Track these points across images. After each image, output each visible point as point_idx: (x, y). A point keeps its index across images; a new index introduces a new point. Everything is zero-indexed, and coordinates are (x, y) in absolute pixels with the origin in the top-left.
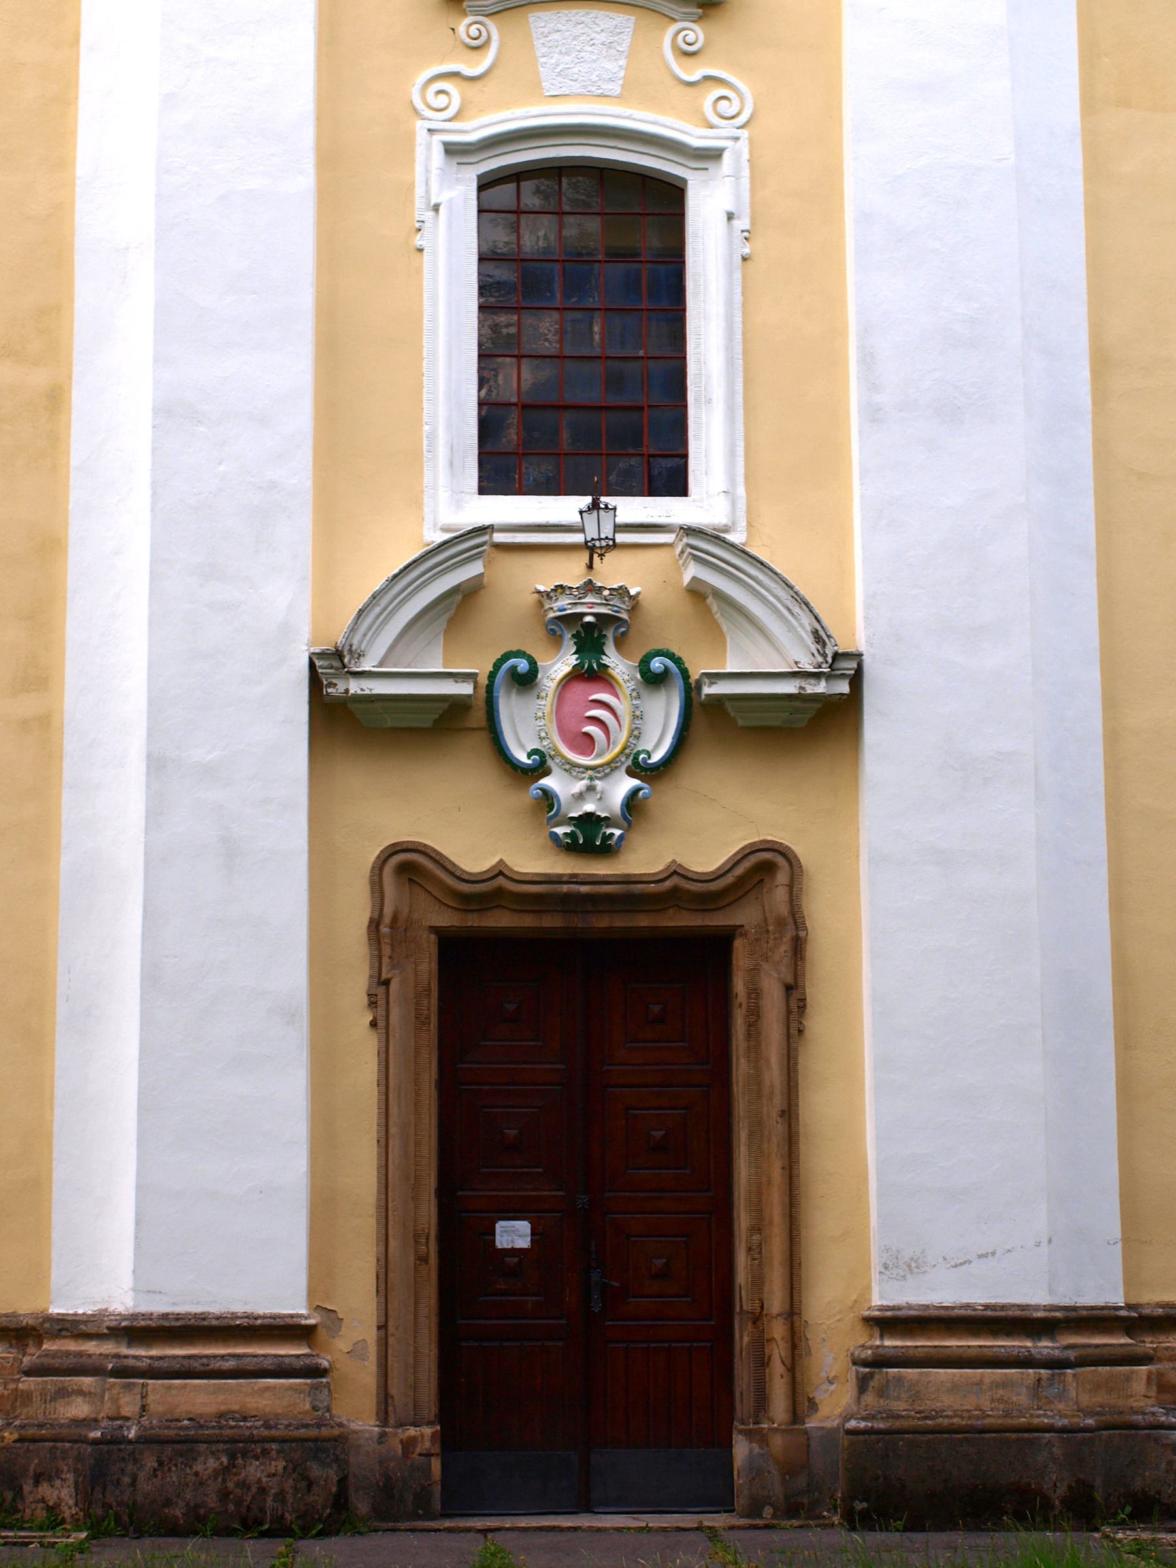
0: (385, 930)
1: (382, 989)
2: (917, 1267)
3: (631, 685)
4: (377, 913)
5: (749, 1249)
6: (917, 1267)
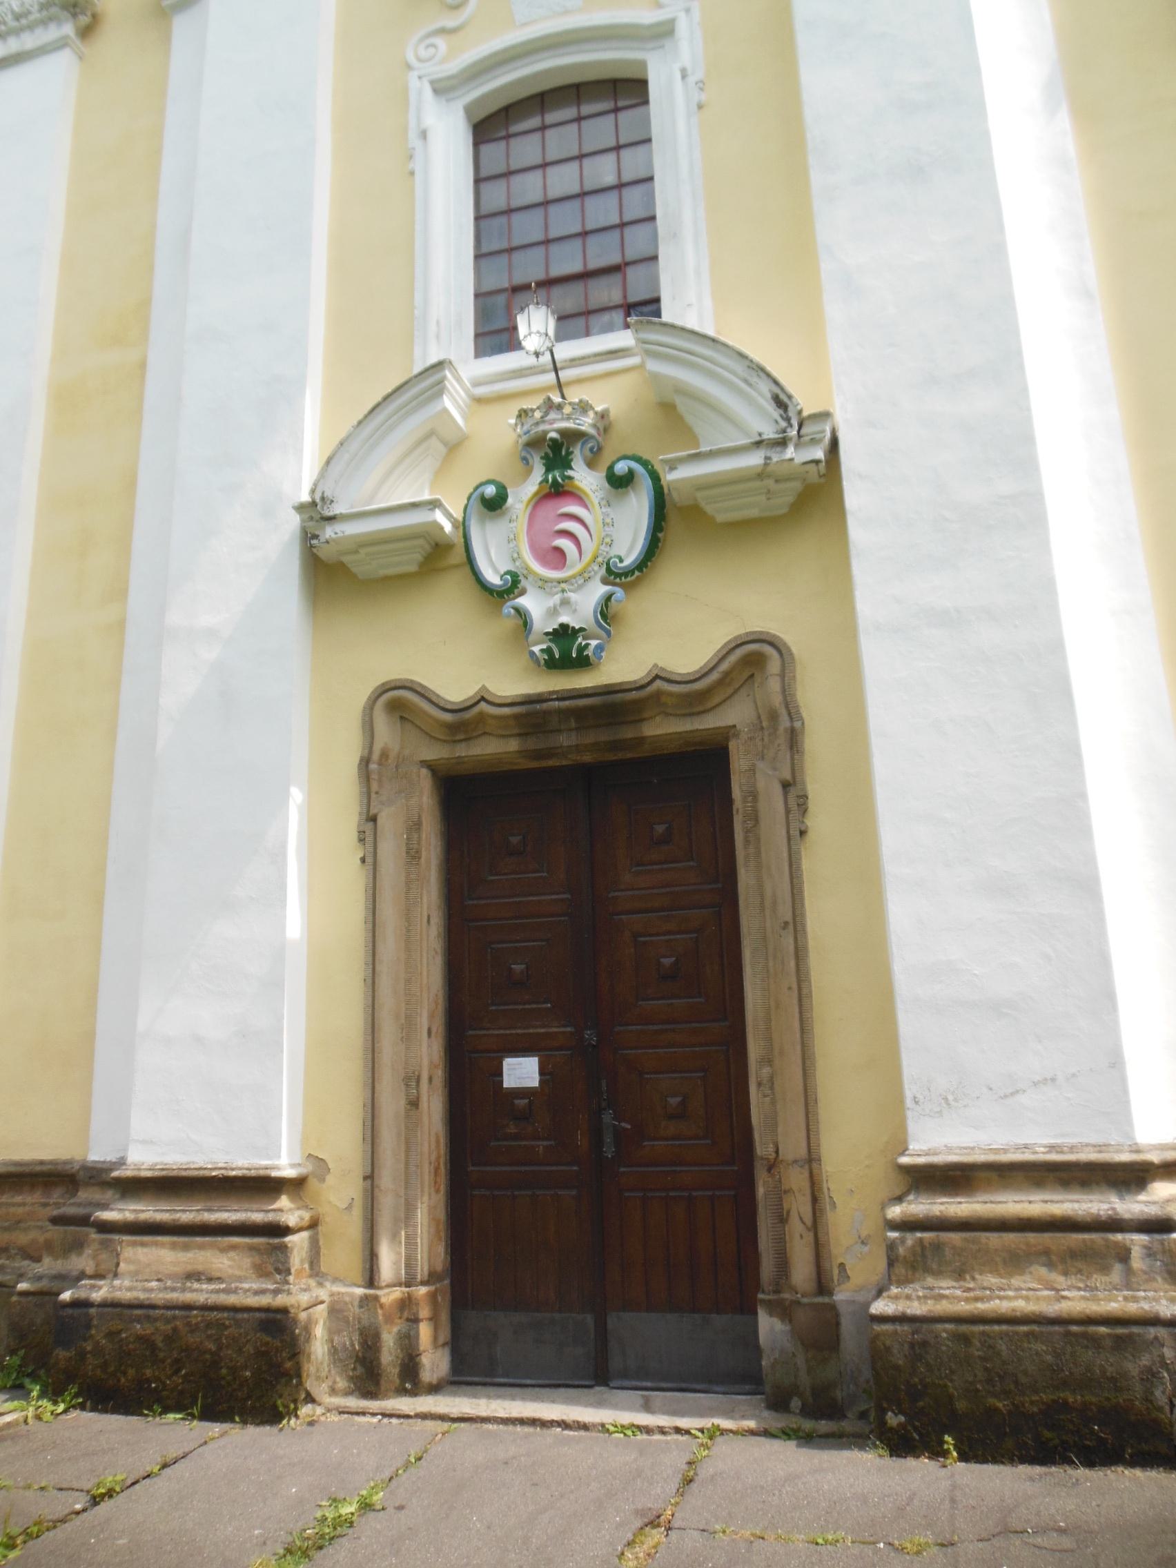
0: (373, 766)
1: (371, 824)
2: (956, 1100)
3: (600, 494)
4: (367, 751)
5: (759, 1084)
6: (956, 1100)
